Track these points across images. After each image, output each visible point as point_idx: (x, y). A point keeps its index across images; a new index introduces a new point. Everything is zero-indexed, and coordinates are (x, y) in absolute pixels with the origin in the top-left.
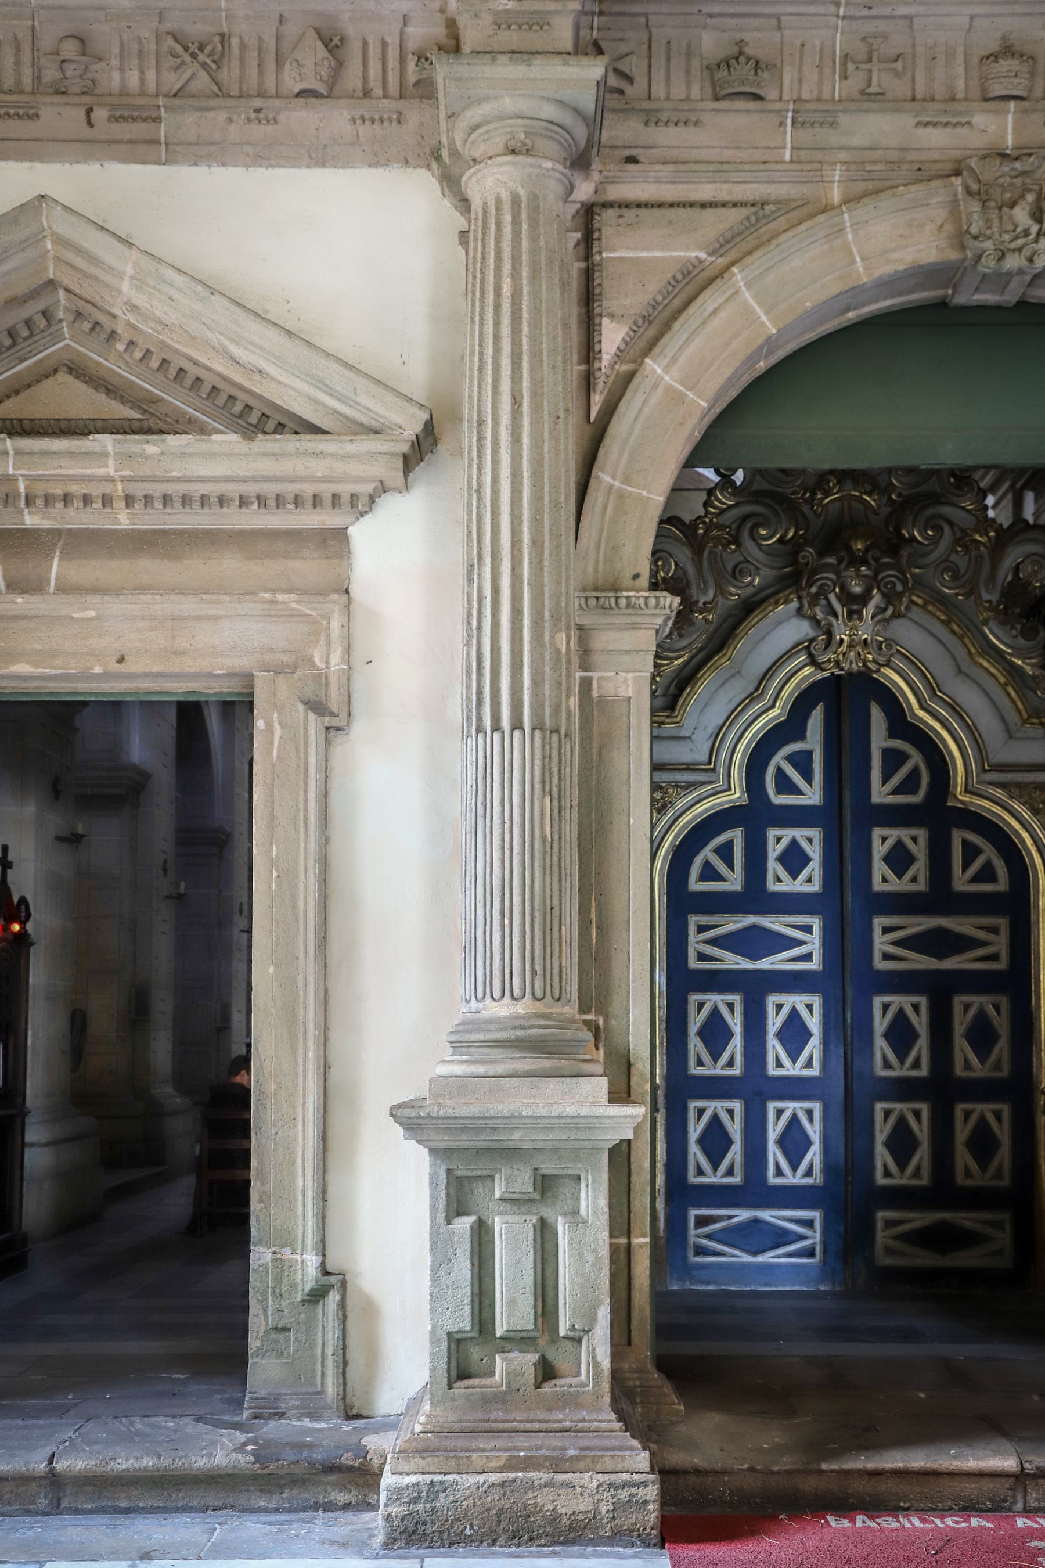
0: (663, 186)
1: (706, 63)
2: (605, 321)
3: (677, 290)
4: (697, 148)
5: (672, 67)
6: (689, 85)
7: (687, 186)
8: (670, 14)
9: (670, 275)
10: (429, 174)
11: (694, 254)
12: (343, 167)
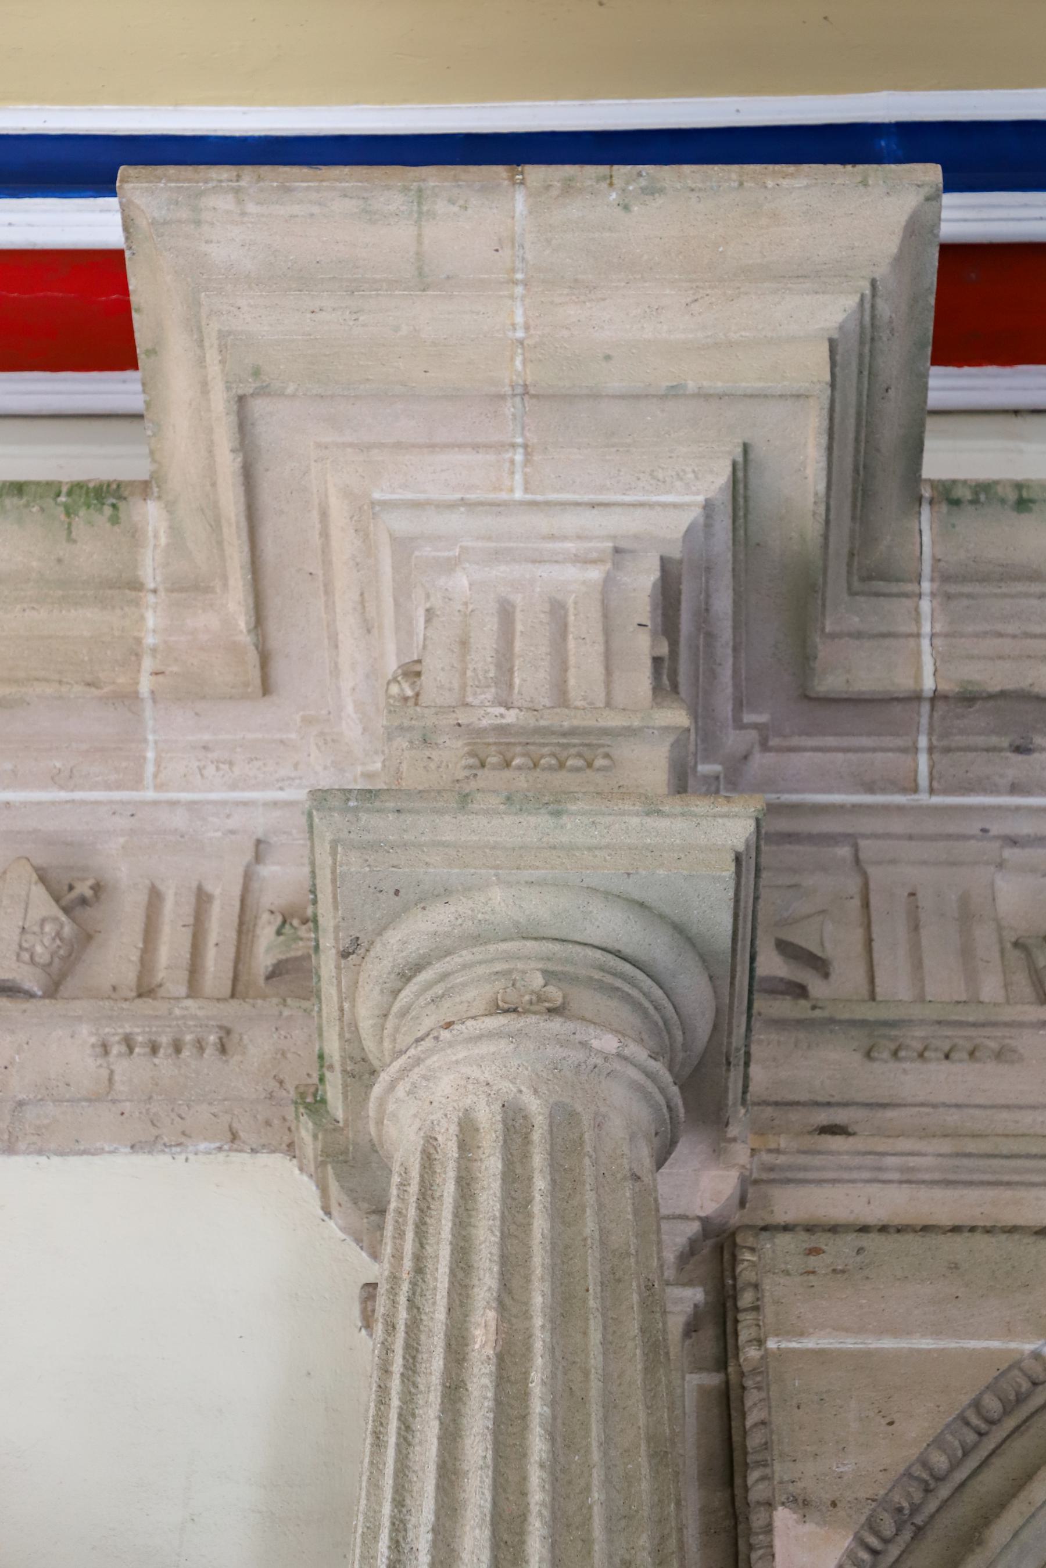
0: (923, 1193)
1: (1010, 937)
2: (783, 1517)
3: (990, 1444)
4: (1007, 1107)
5: (924, 942)
6: (971, 977)
7: (991, 1193)
8: (910, 837)
9: (966, 1399)
10: (292, 1166)
11: (1028, 1347)
12: (61, 1153)
